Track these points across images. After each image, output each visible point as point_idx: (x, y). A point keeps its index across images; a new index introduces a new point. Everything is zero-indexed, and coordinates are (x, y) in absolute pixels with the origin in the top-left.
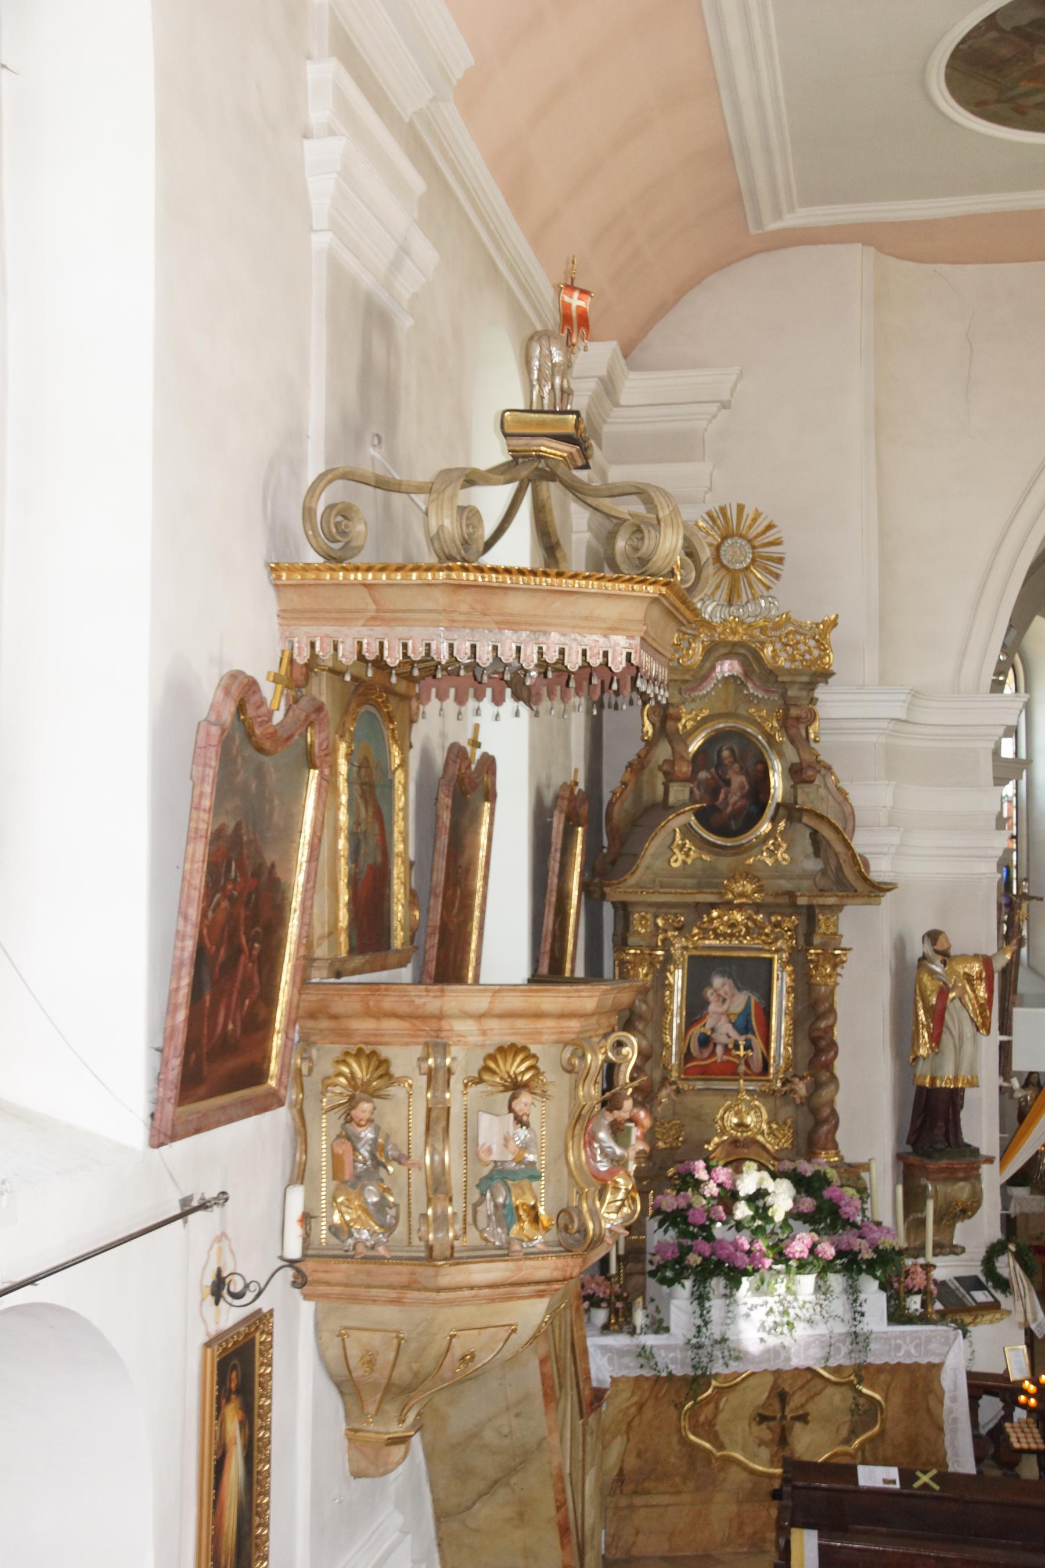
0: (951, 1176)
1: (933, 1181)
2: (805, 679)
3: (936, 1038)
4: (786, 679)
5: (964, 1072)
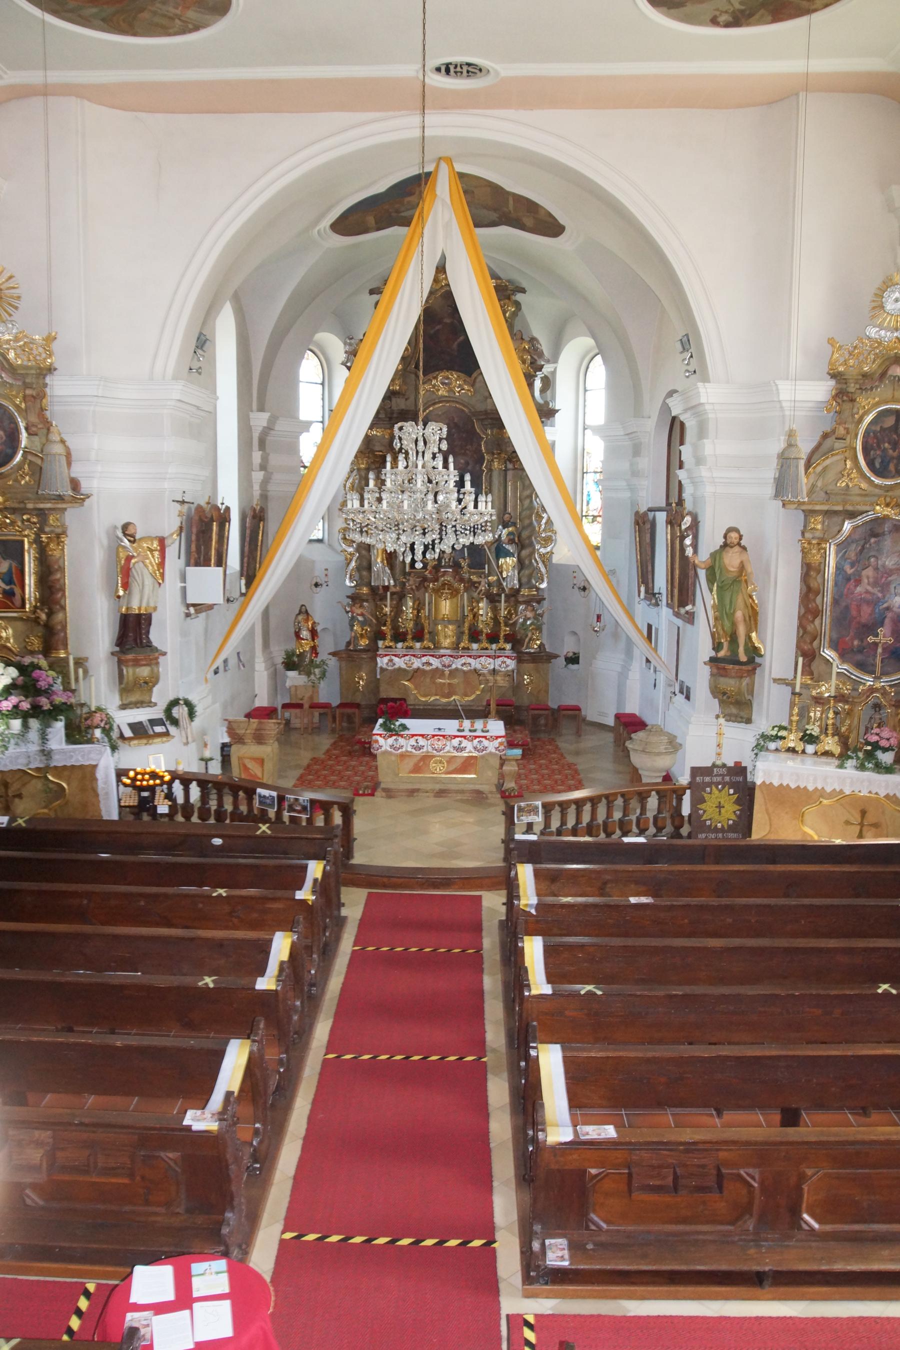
0: (137, 663)
1: (127, 666)
2: (33, 372)
3: (126, 586)
4: (22, 372)
5: (144, 605)
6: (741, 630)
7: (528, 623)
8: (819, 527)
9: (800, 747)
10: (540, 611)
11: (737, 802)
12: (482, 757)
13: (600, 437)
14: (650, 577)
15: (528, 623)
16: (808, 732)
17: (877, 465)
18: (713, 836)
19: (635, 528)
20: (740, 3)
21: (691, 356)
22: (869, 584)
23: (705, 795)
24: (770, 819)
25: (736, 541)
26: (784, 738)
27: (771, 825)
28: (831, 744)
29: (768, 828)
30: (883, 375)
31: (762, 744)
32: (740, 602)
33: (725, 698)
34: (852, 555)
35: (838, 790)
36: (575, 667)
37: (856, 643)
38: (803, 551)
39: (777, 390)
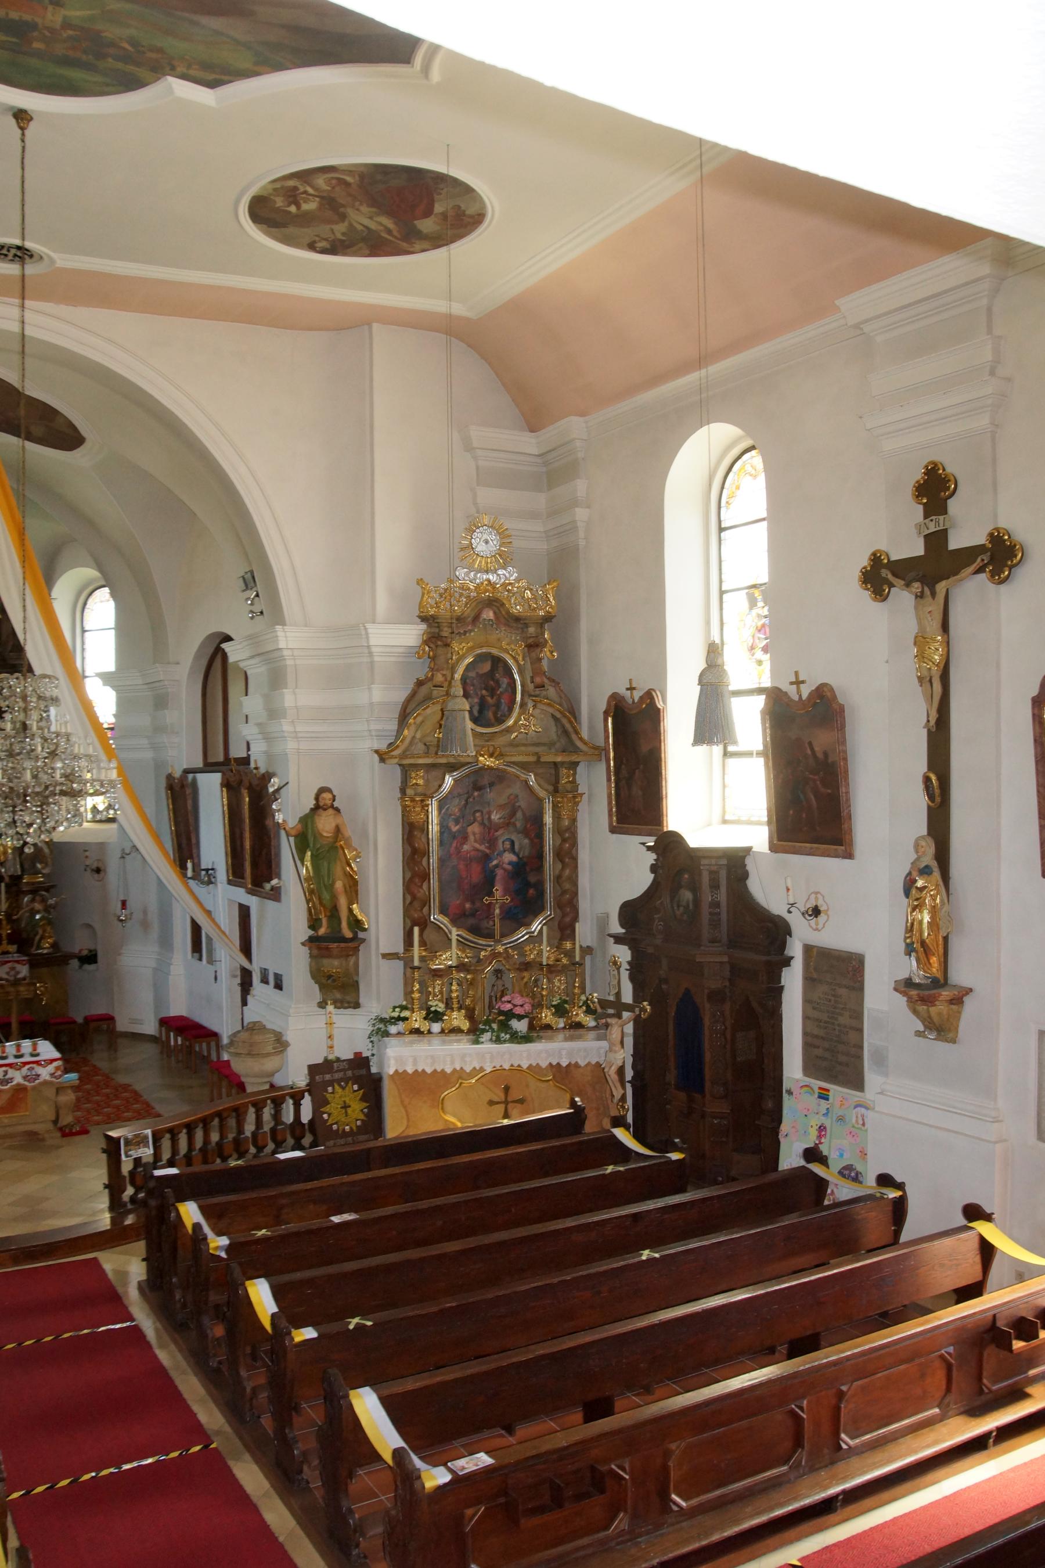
6: (343, 902)
7: (38, 917)
8: (421, 782)
9: (425, 1026)
10: (51, 902)
11: (363, 1099)
12: (34, 1088)
13: (111, 687)
14: (194, 851)
15: (38, 917)
16: (433, 1009)
18: (342, 1141)
21: (257, 595)
22: (476, 841)
23: (328, 1096)
24: (407, 1111)
25: (329, 802)
26: (405, 1019)
27: (408, 1120)
28: (458, 1019)
29: (405, 1122)
30: (476, 618)
31: (382, 1028)
32: (338, 870)
33: (329, 981)
35: (478, 1068)
36: (92, 967)
37: (468, 905)
38: (404, 808)
39: (367, 634)
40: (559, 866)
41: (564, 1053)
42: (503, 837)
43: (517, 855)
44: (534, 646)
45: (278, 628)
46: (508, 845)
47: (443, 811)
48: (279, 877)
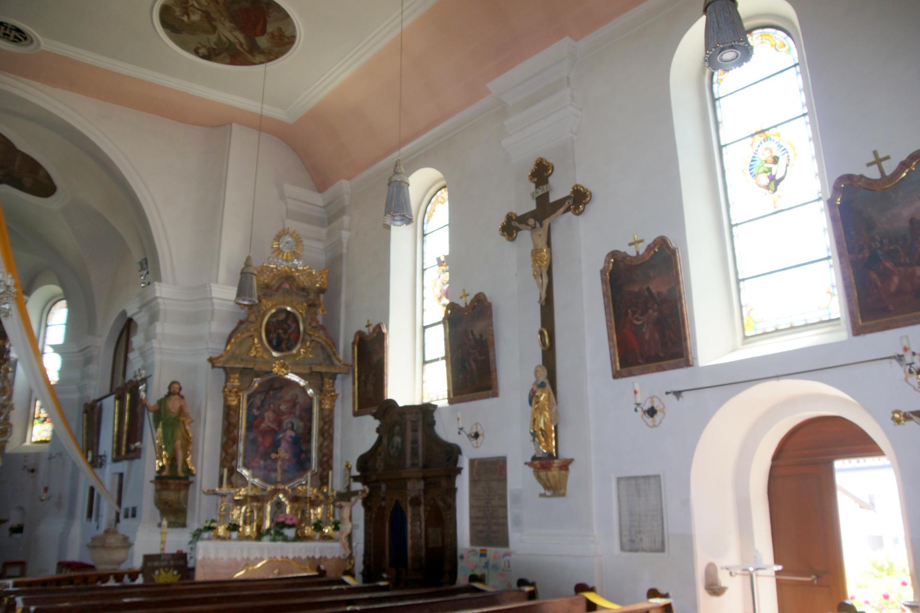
6: (180, 454)
17: (274, 342)
19: (83, 416)
20: (215, 44)
21: (148, 273)
25: (177, 391)
34: (257, 401)
39: (211, 290)
40: (322, 439)
41: (317, 550)
42: (287, 421)
43: (295, 431)
44: (312, 306)
45: (156, 283)
46: (290, 425)
47: (250, 402)
48: (141, 440)
